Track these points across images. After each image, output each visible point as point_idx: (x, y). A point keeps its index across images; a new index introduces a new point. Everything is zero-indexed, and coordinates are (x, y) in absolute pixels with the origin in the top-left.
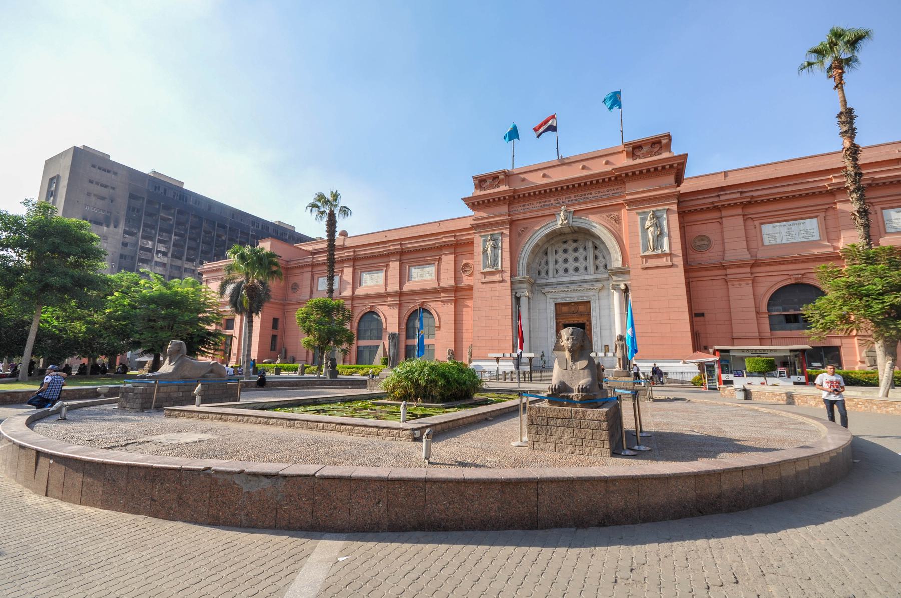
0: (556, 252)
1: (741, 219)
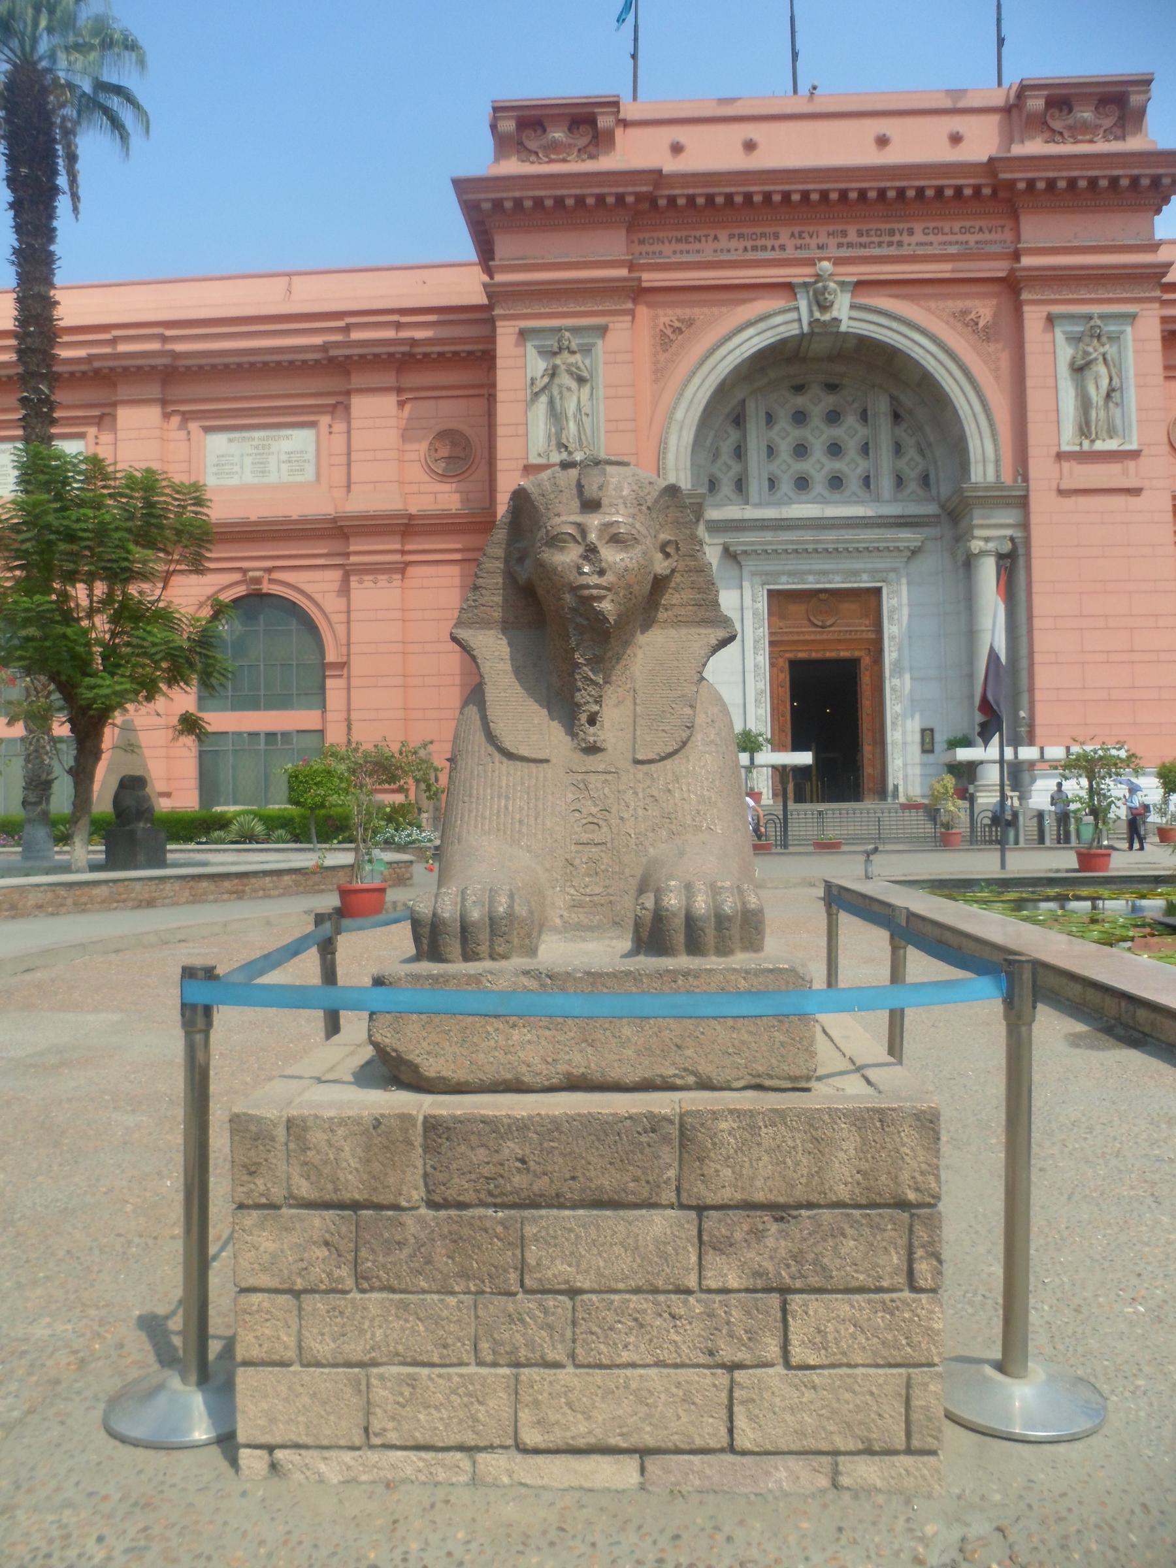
0: (770, 419)
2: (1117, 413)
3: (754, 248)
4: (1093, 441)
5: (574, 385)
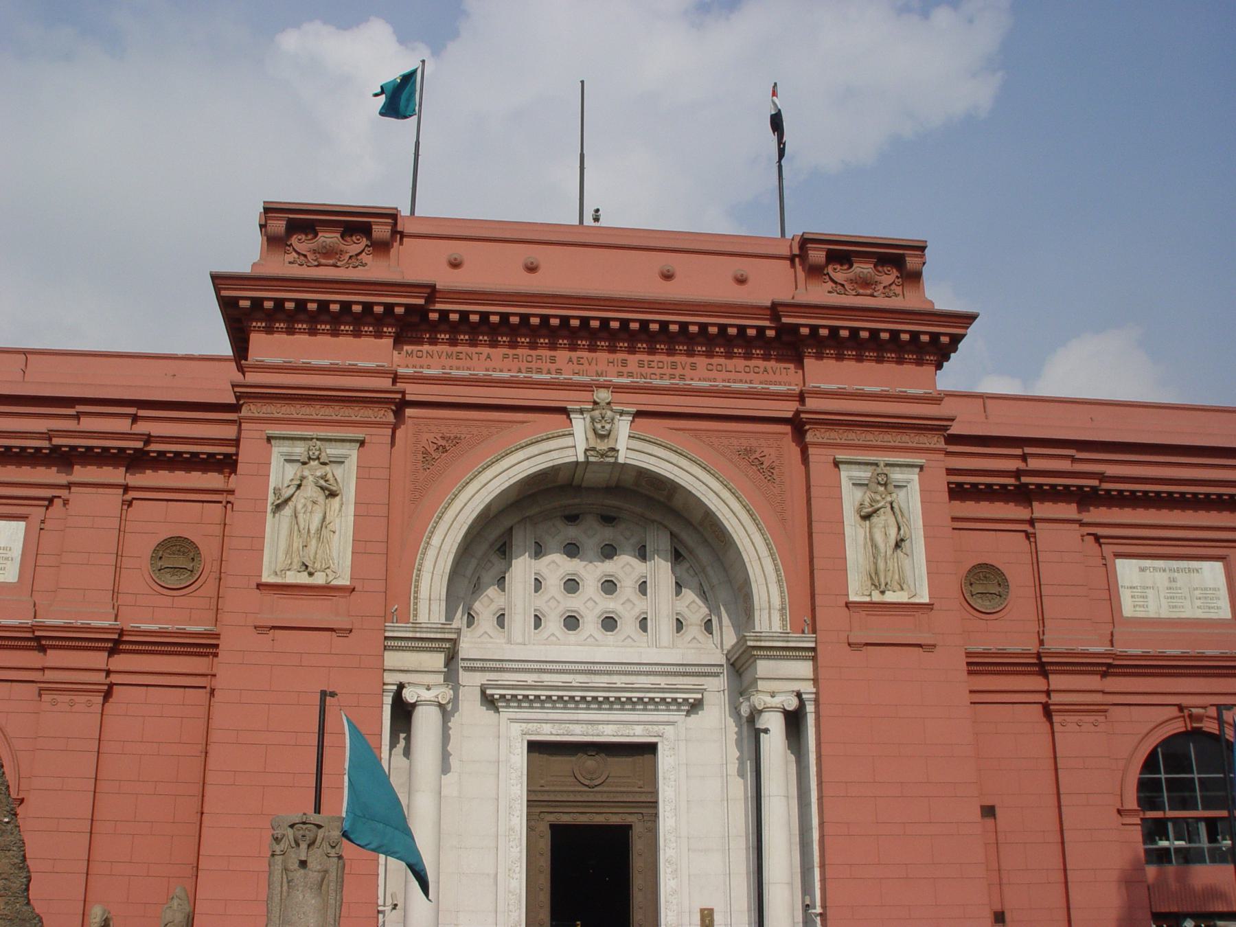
1: (1074, 531)
2: (906, 562)
3: (529, 370)
4: (883, 593)
5: (320, 496)
